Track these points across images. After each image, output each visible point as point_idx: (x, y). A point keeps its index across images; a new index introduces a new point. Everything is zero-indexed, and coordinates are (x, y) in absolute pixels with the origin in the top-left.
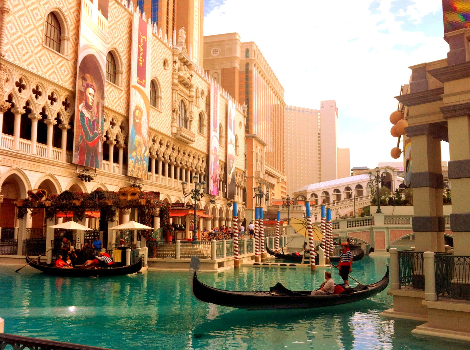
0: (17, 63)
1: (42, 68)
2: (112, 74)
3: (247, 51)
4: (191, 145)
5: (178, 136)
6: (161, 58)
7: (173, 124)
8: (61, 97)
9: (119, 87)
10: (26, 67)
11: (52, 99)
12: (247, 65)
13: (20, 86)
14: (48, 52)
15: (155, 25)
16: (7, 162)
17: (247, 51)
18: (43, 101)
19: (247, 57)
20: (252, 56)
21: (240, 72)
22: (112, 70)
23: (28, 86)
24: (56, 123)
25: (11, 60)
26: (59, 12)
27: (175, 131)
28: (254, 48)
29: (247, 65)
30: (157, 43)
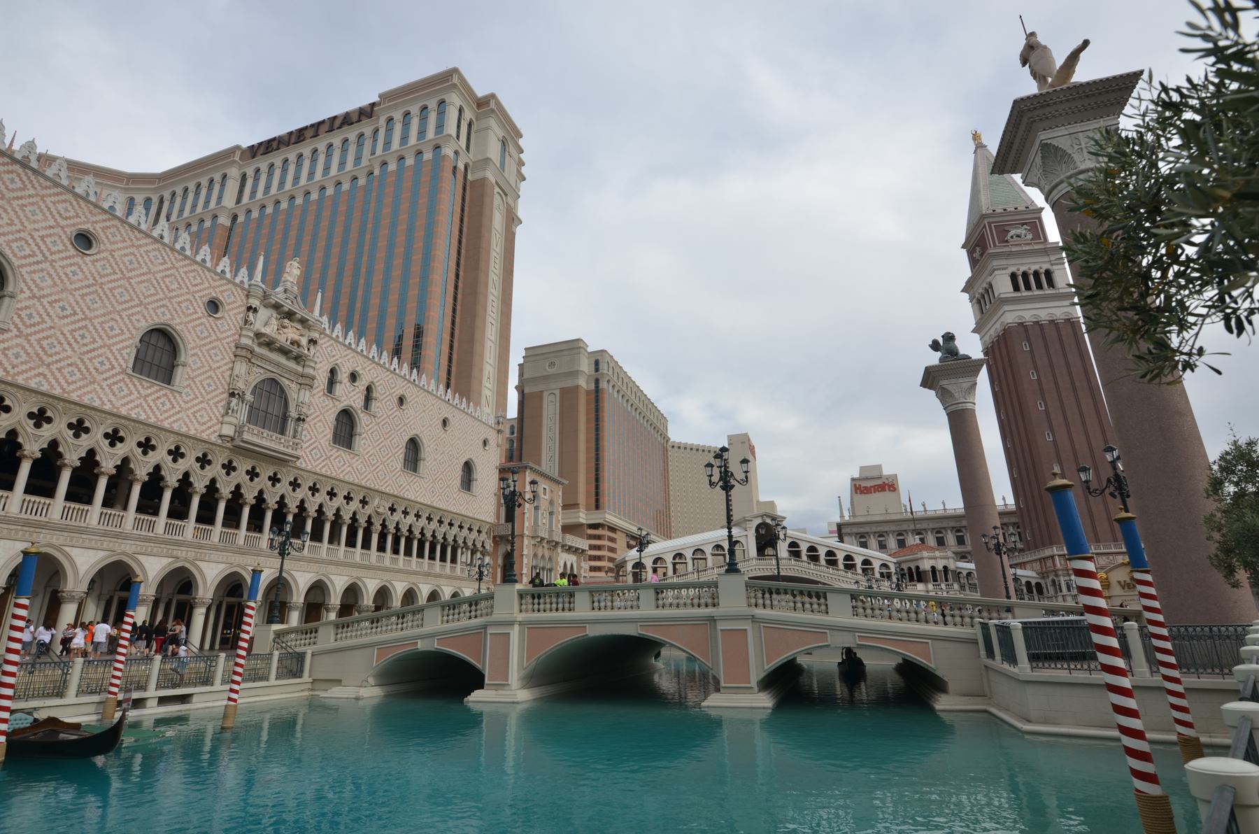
3: (597, 363)
4: (298, 464)
5: (238, 442)
7: (226, 419)
12: (597, 381)
17: (597, 363)
19: (597, 370)
20: (604, 368)
21: (588, 392)
27: (228, 430)
28: (607, 359)
29: (597, 381)
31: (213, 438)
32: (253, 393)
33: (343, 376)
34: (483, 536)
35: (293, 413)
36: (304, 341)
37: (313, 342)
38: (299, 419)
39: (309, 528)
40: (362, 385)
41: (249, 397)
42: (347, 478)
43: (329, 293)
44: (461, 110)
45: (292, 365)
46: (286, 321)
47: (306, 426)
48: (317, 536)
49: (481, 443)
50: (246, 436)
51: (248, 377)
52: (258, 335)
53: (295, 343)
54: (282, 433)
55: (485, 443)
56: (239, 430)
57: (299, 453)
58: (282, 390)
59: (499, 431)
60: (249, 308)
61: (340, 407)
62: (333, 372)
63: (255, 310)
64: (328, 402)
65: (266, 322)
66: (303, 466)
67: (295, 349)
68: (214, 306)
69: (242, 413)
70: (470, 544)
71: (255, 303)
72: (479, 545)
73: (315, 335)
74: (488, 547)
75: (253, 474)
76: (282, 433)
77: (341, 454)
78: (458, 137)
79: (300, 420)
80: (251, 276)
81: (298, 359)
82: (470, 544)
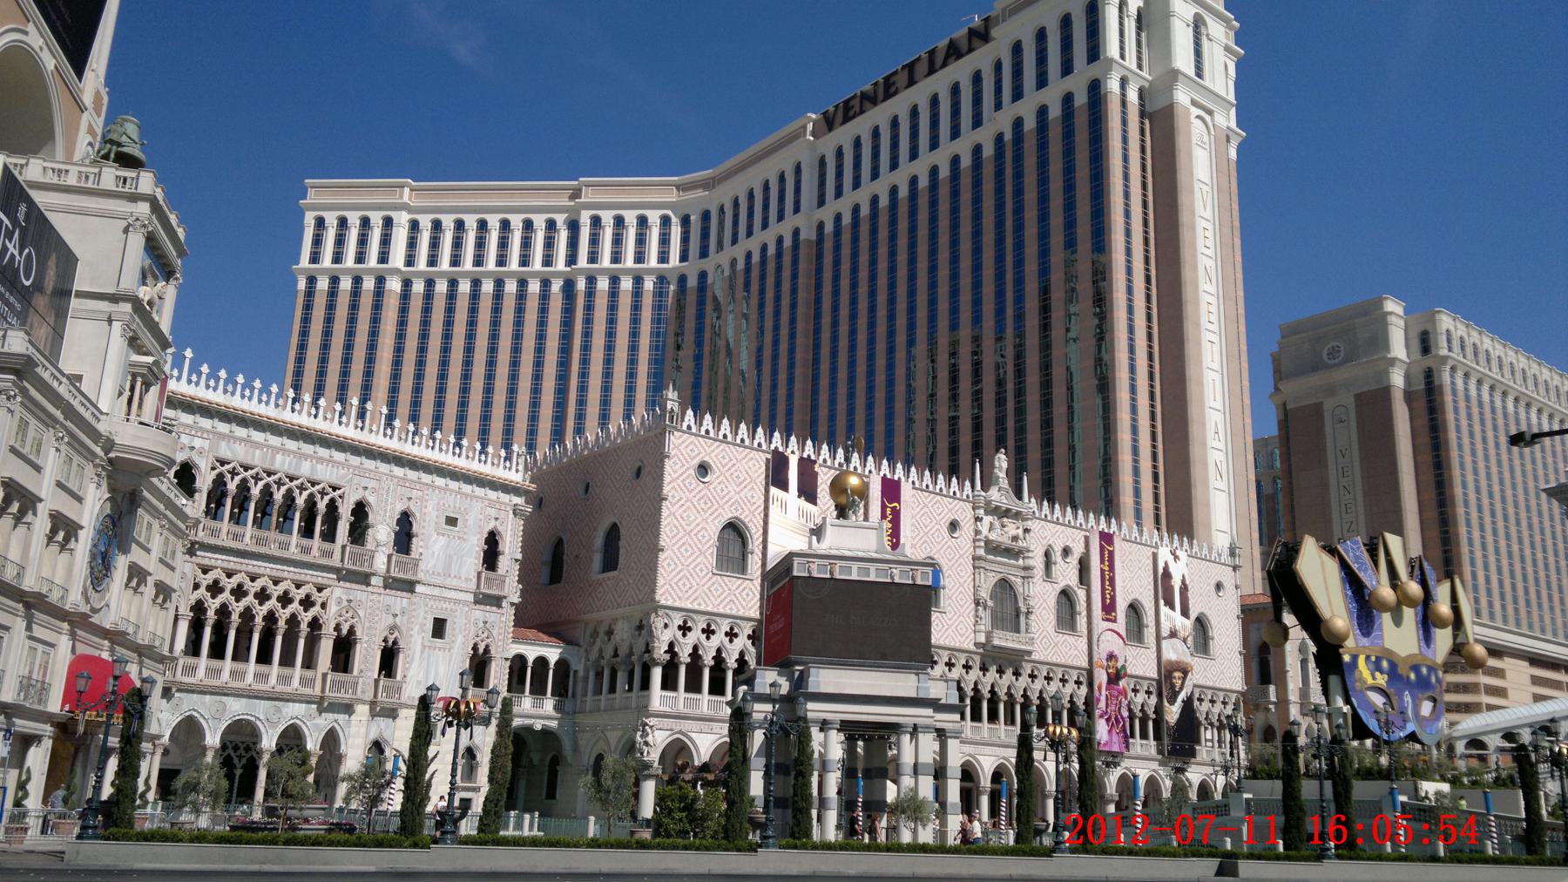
0: (677, 604)
8: (747, 629)
25: (669, 603)
31: (972, 648)
33: (1057, 556)
35: (1023, 609)
36: (1020, 532)
40: (1073, 560)
41: (990, 603)
43: (1038, 476)
47: (1032, 617)
49: (1213, 583)
50: (996, 642)
51: (988, 582)
52: (988, 542)
53: (1015, 538)
54: (1018, 631)
55: (1219, 586)
56: (989, 635)
59: (1235, 568)
61: (1059, 588)
62: (1047, 555)
64: (1048, 586)
68: (954, 526)
69: (986, 616)
70: (1214, 720)
76: (1018, 631)
80: (973, 487)
82: (1214, 720)
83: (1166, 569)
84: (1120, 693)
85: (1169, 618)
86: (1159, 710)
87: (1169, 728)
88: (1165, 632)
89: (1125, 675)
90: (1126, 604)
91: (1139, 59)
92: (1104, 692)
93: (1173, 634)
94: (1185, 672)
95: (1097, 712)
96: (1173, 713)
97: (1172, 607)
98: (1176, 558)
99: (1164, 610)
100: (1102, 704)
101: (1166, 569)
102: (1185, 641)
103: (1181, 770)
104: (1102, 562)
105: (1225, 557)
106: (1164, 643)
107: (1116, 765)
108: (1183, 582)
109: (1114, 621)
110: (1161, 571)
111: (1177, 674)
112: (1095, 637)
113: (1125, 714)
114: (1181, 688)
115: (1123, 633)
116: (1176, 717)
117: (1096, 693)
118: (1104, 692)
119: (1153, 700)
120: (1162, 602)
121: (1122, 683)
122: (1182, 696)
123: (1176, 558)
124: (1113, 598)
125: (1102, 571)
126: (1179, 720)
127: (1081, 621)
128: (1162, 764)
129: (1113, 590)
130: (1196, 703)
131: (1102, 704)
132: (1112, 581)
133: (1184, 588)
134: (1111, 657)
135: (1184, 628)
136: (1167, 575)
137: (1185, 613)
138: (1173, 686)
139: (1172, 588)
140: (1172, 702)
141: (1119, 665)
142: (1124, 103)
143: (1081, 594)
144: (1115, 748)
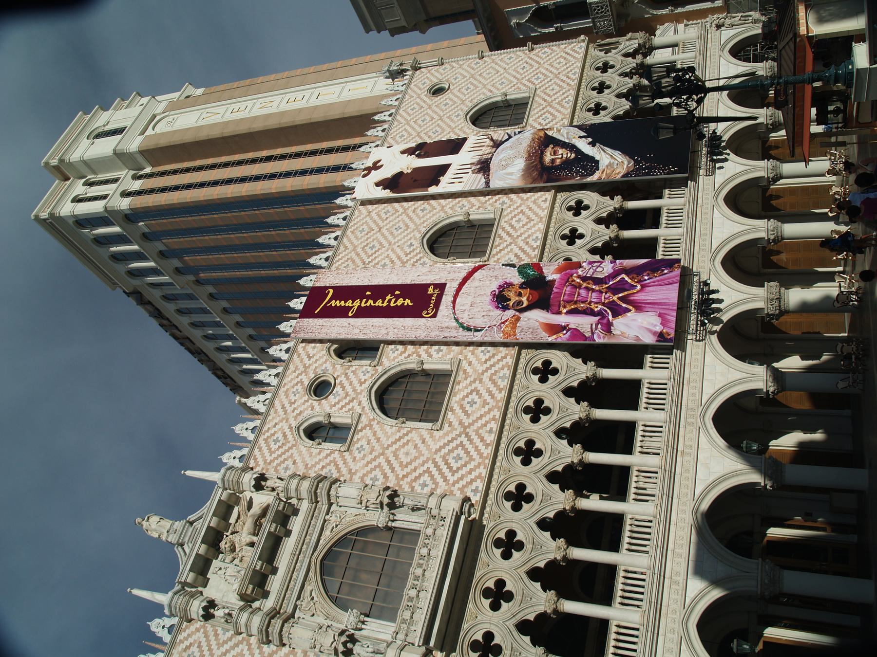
1: (532, 223)
2: (510, 112)
6: (430, 102)
9: (532, 96)
10: (503, 392)
11: (578, 208)
13: (573, 237)
14: (459, 383)
15: (376, 118)
16: (704, 245)
18: (585, 224)
22: (504, 113)
23: (537, 394)
24: (619, 197)
26: (375, 406)
30: (414, 92)
32: (343, 606)
34: (614, 58)
36: (261, 499)
37: (260, 483)
38: (392, 506)
39: (594, 503)
42: (504, 384)
44: (77, 200)
45: (296, 524)
46: (222, 545)
48: (615, 482)
55: (437, 91)
57: (451, 506)
58: (341, 542)
59: (416, 68)
60: (208, 616)
62: (314, 432)
63: (212, 604)
64: (361, 439)
65: (225, 583)
66: (480, 485)
67: (268, 526)
71: (196, 607)
72: (632, 63)
73: (248, 479)
74: (634, 45)
75: (498, 595)
77: (458, 396)
78: (104, 197)
79: (392, 501)
81: (284, 518)
83: (385, 184)
84: (567, 280)
85: (458, 177)
86: (607, 189)
87: (637, 171)
88: (476, 182)
89: (537, 267)
90: (429, 258)
91: (106, 182)
92: (562, 319)
93: (484, 167)
94: (546, 141)
95: (600, 338)
96: (612, 163)
97: (443, 169)
98: (376, 166)
99: (445, 185)
100: (584, 323)
101: (385, 184)
102: (497, 145)
103: (715, 146)
104: (342, 313)
105: (399, 83)
106: (496, 183)
107: (706, 291)
108: (410, 152)
109: (441, 287)
110: (387, 193)
111: (548, 157)
112: (464, 336)
113: (607, 267)
114: (572, 147)
115: (468, 264)
116: (618, 156)
117: (563, 337)
118: (562, 319)
119: (589, 198)
120: (433, 190)
121: (551, 273)
122: (584, 146)
123: (376, 166)
124: (406, 290)
125: (362, 313)
126: (625, 152)
127: (436, 360)
128: (704, 183)
129: (389, 289)
130: (604, 118)
131: (584, 323)
132: (379, 291)
133: (422, 150)
134: (500, 299)
135: (478, 146)
136: (394, 183)
137: (454, 146)
138: (567, 164)
139: (417, 170)
140: (592, 164)
141: (517, 280)
142: (139, 193)
143: (394, 360)
144: (670, 294)
